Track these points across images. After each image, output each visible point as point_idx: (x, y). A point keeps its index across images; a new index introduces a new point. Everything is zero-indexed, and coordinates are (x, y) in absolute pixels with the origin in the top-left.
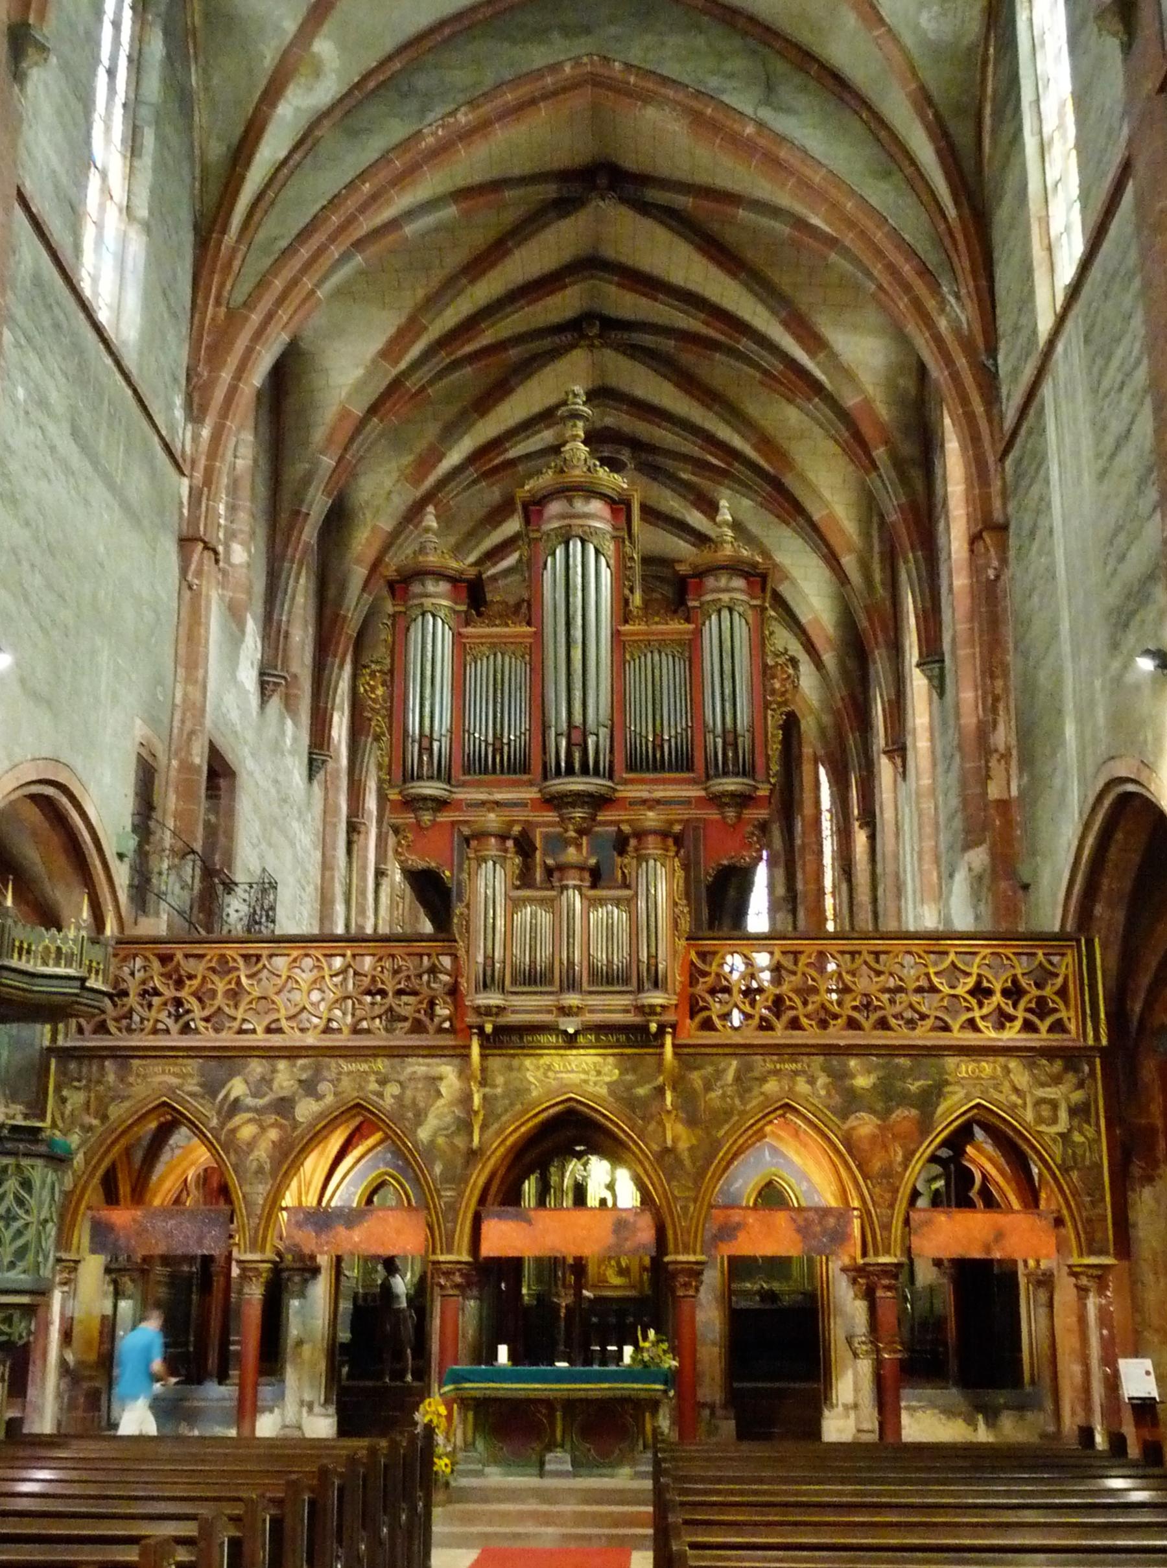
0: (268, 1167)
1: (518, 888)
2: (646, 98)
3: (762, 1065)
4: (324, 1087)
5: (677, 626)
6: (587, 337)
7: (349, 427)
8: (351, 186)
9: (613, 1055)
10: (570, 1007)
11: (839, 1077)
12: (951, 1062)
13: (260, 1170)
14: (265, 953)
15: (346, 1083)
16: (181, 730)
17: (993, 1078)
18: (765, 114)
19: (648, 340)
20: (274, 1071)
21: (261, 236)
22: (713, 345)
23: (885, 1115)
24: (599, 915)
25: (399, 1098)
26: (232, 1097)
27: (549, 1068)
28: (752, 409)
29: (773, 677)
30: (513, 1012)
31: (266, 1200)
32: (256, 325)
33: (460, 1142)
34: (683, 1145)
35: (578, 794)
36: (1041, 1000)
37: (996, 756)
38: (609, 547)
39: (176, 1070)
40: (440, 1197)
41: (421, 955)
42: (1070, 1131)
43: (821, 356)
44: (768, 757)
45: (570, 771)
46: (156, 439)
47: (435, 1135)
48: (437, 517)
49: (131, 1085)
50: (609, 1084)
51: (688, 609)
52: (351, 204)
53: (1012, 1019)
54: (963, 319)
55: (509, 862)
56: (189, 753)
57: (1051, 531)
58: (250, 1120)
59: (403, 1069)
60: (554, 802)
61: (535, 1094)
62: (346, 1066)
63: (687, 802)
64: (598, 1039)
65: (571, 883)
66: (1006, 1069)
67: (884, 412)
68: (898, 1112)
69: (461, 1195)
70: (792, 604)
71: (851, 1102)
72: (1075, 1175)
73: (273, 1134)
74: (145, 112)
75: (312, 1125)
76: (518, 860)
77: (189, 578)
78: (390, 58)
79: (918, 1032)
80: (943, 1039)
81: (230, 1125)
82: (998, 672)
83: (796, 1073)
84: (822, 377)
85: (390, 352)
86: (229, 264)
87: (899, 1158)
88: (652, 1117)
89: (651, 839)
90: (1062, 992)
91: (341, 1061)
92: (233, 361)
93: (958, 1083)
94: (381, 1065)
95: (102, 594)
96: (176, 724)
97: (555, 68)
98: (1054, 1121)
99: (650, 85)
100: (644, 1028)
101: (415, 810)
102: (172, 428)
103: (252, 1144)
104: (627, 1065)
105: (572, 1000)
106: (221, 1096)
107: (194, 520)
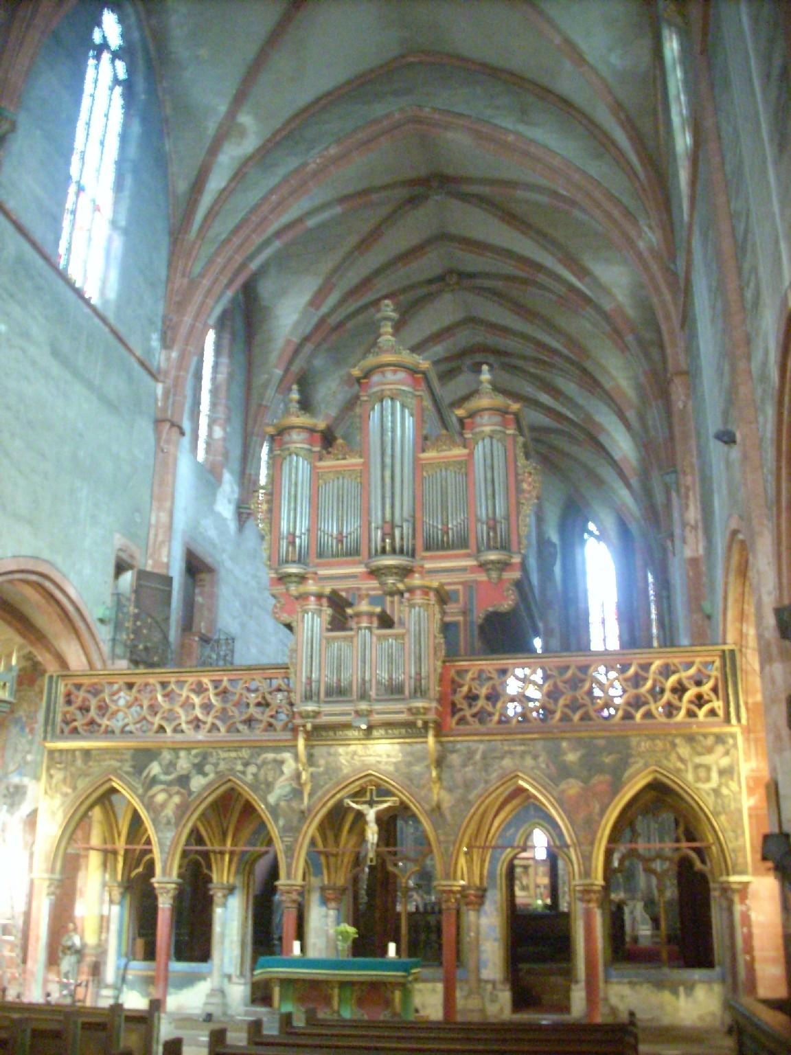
0: (173, 821)
1: (329, 630)
2: (447, 127)
4: (208, 768)
5: (459, 452)
6: (448, 285)
7: (291, 348)
8: (265, 199)
9: (399, 743)
10: (362, 710)
13: (168, 823)
14: (173, 680)
16: (155, 541)
17: (664, 750)
18: (521, 128)
19: (488, 283)
20: (178, 757)
21: (211, 233)
22: (525, 282)
23: (585, 781)
25: (255, 775)
26: (152, 774)
27: (355, 753)
28: (562, 322)
29: (522, 481)
30: (326, 715)
31: (172, 843)
32: (206, 288)
34: (446, 805)
35: (387, 567)
37: (688, 528)
38: (412, 402)
39: (118, 757)
40: (283, 841)
41: (270, 679)
42: (720, 785)
43: (587, 279)
44: (519, 535)
45: (384, 551)
46: (133, 360)
47: (279, 799)
49: (90, 767)
50: (395, 764)
51: (465, 439)
52: (265, 208)
54: (654, 240)
55: (323, 614)
56: (160, 556)
58: (163, 790)
59: (259, 755)
60: (375, 573)
61: (345, 771)
62: (223, 755)
63: (463, 569)
64: (387, 733)
65: (364, 625)
66: (674, 745)
67: (631, 312)
68: (596, 777)
69: (296, 840)
70: (607, 446)
71: (565, 772)
72: (723, 818)
73: (177, 799)
74: (128, 165)
75: (199, 794)
76: (329, 611)
77: (162, 444)
81: (151, 793)
82: (688, 470)
84: (588, 293)
85: (315, 302)
86: (190, 254)
87: (597, 807)
88: (424, 786)
89: (418, 592)
90: (715, 690)
91: (220, 752)
92: (192, 309)
93: (640, 755)
94: (245, 753)
95: (81, 454)
96: (152, 536)
97: (387, 116)
98: (708, 779)
99: (449, 119)
101: (285, 584)
102: (149, 351)
103: (163, 805)
105: (363, 706)
106: (145, 774)
107: (164, 409)
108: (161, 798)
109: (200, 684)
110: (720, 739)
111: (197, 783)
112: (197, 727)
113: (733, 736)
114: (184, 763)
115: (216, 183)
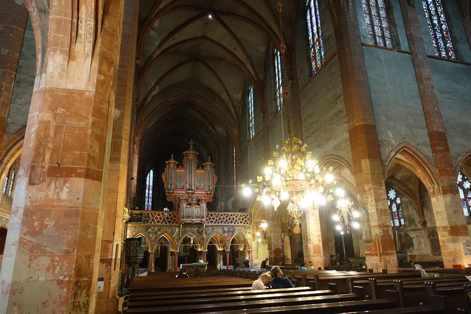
3: (215, 227)
4: (161, 230)
5: (203, 171)
11: (223, 229)
12: (236, 227)
13: (153, 240)
15: (164, 230)
23: (228, 234)
24: (197, 209)
25: (171, 232)
33: (178, 237)
35: (191, 193)
36: (246, 220)
47: (175, 236)
48: (173, 155)
53: (242, 222)
57: (248, 164)
60: (187, 193)
63: (204, 194)
66: (242, 228)
71: (224, 232)
73: (155, 236)
78: (164, 88)
79: (232, 224)
80: (235, 224)
83: (218, 228)
90: (248, 219)
94: (168, 227)
98: (247, 234)
100: (202, 223)
101: (169, 194)
103: (152, 237)
104: (199, 227)
105: (194, 220)
108: (151, 236)
109: (159, 214)
110: (249, 227)
111: (159, 233)
112: (158, 223)
113: (251, 227)
114: (156, 229)
115: (149, 100)
